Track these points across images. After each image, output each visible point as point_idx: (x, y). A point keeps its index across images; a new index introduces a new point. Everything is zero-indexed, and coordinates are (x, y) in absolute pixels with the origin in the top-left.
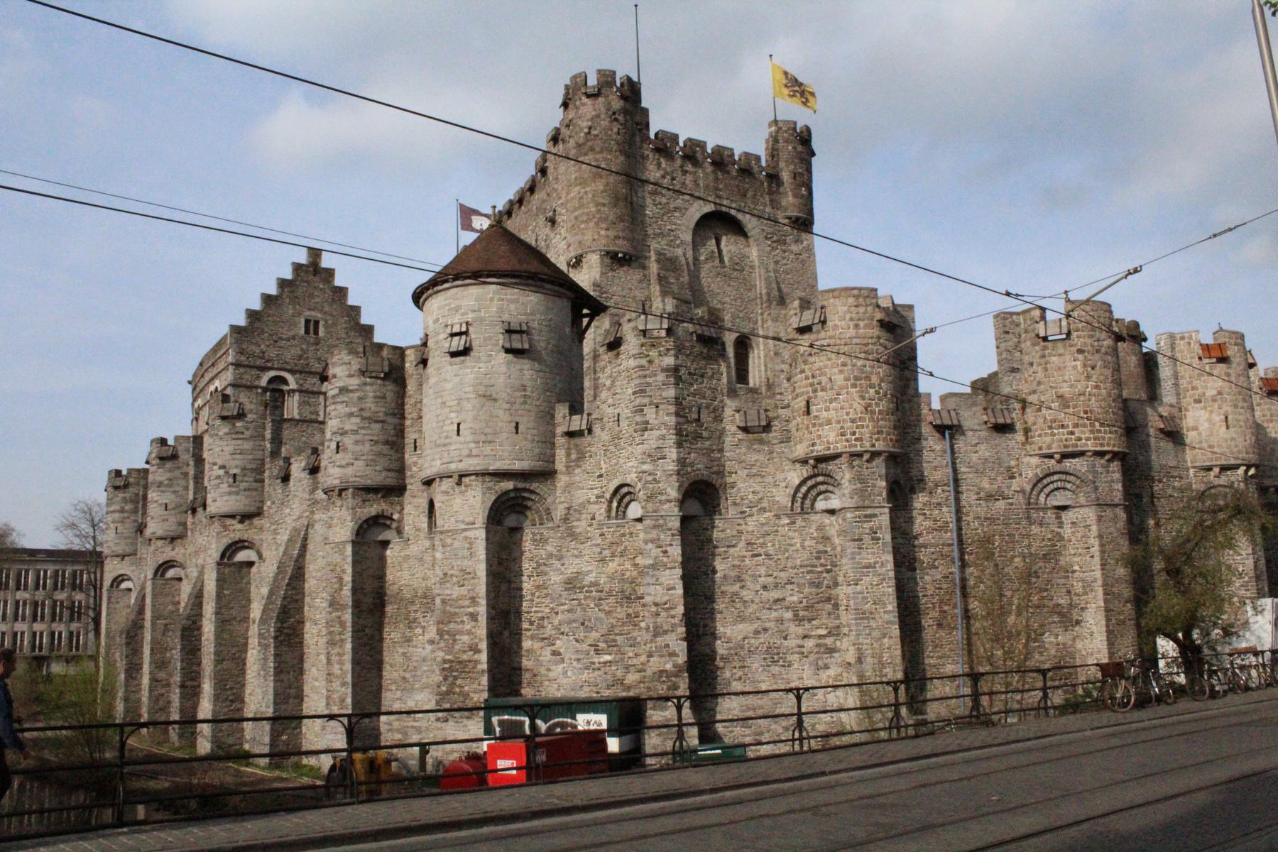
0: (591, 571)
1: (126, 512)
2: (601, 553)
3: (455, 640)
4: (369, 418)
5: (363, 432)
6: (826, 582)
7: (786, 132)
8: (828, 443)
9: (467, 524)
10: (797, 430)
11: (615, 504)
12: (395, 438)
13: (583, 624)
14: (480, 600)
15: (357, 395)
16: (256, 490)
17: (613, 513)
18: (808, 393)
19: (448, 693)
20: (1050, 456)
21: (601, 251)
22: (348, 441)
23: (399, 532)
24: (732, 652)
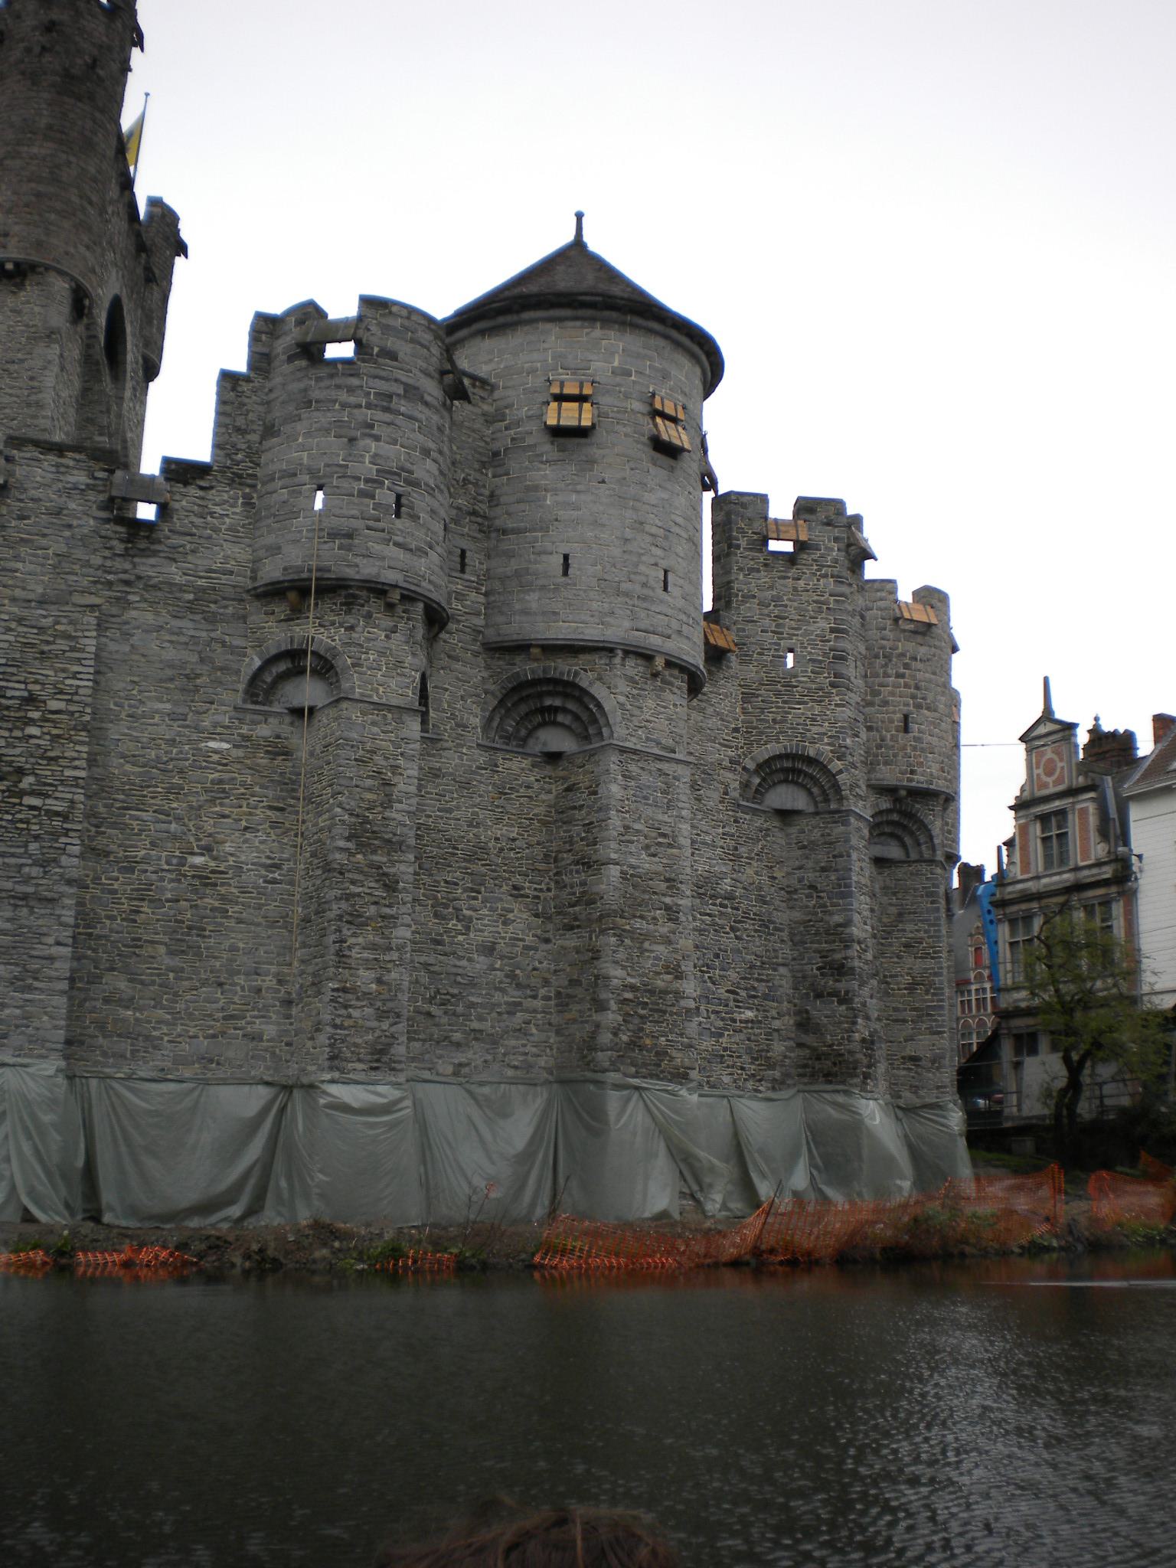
3: (642, 951)
8: (931, 775)
10: (879, 747)
11: (757, 781)
14: (683, 887)
17: (751, 793)
19: (633, 1044)
21: (73, 279)
22: (420, 501)
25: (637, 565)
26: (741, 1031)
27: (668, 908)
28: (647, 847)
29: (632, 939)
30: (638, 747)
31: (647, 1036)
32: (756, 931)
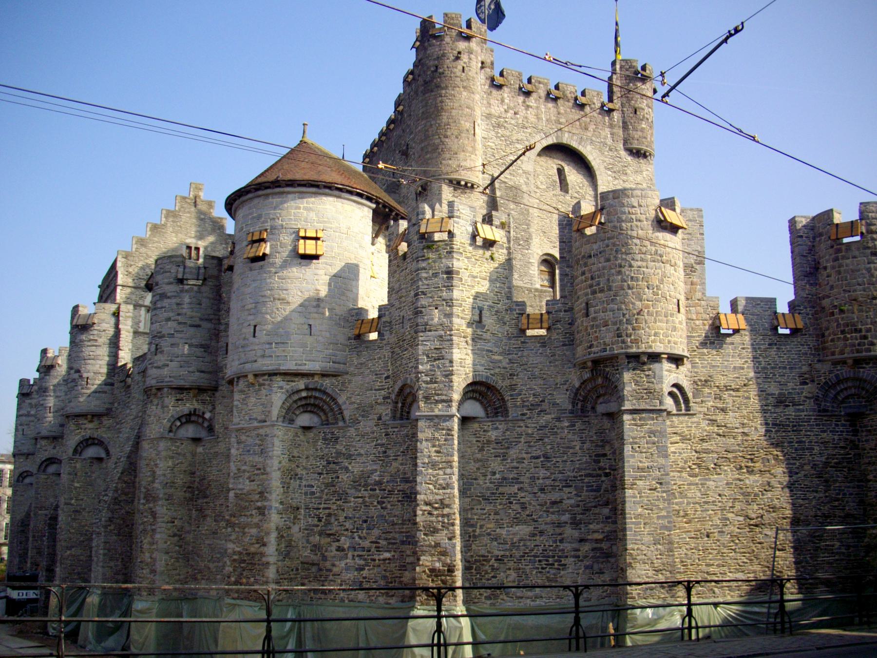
0: (376, 470)
1: (32, 416)
2: (385, 452)
3: (244, 533)
4: (185, 323)
5: (179, 335)
6: (604, 486)
7: (627, 70)
8: (605, 344)
9: (261, 421)
11: (400, 405)
12: (208, 342)
13: (365, 521)
15: (174, 301)
16: (105, 392)
18: (587, 294)
20: (844, 362)
21: (444, 179)
22: (165, 344)
23: (211, 429)
24: (508, 553)
25: (241, 330)
26: (379, 566)
27: (259, 508)
28: (249, 478)
29: (239, 528)
30: (246, 425)
31: (244, 577)
32: (399, 501)
